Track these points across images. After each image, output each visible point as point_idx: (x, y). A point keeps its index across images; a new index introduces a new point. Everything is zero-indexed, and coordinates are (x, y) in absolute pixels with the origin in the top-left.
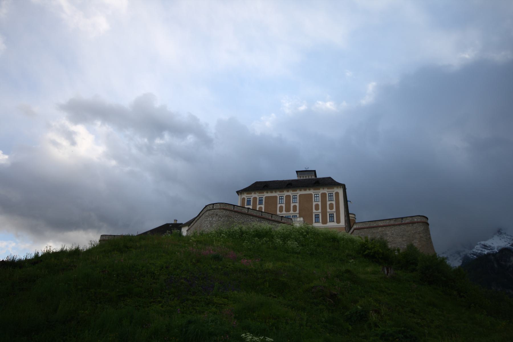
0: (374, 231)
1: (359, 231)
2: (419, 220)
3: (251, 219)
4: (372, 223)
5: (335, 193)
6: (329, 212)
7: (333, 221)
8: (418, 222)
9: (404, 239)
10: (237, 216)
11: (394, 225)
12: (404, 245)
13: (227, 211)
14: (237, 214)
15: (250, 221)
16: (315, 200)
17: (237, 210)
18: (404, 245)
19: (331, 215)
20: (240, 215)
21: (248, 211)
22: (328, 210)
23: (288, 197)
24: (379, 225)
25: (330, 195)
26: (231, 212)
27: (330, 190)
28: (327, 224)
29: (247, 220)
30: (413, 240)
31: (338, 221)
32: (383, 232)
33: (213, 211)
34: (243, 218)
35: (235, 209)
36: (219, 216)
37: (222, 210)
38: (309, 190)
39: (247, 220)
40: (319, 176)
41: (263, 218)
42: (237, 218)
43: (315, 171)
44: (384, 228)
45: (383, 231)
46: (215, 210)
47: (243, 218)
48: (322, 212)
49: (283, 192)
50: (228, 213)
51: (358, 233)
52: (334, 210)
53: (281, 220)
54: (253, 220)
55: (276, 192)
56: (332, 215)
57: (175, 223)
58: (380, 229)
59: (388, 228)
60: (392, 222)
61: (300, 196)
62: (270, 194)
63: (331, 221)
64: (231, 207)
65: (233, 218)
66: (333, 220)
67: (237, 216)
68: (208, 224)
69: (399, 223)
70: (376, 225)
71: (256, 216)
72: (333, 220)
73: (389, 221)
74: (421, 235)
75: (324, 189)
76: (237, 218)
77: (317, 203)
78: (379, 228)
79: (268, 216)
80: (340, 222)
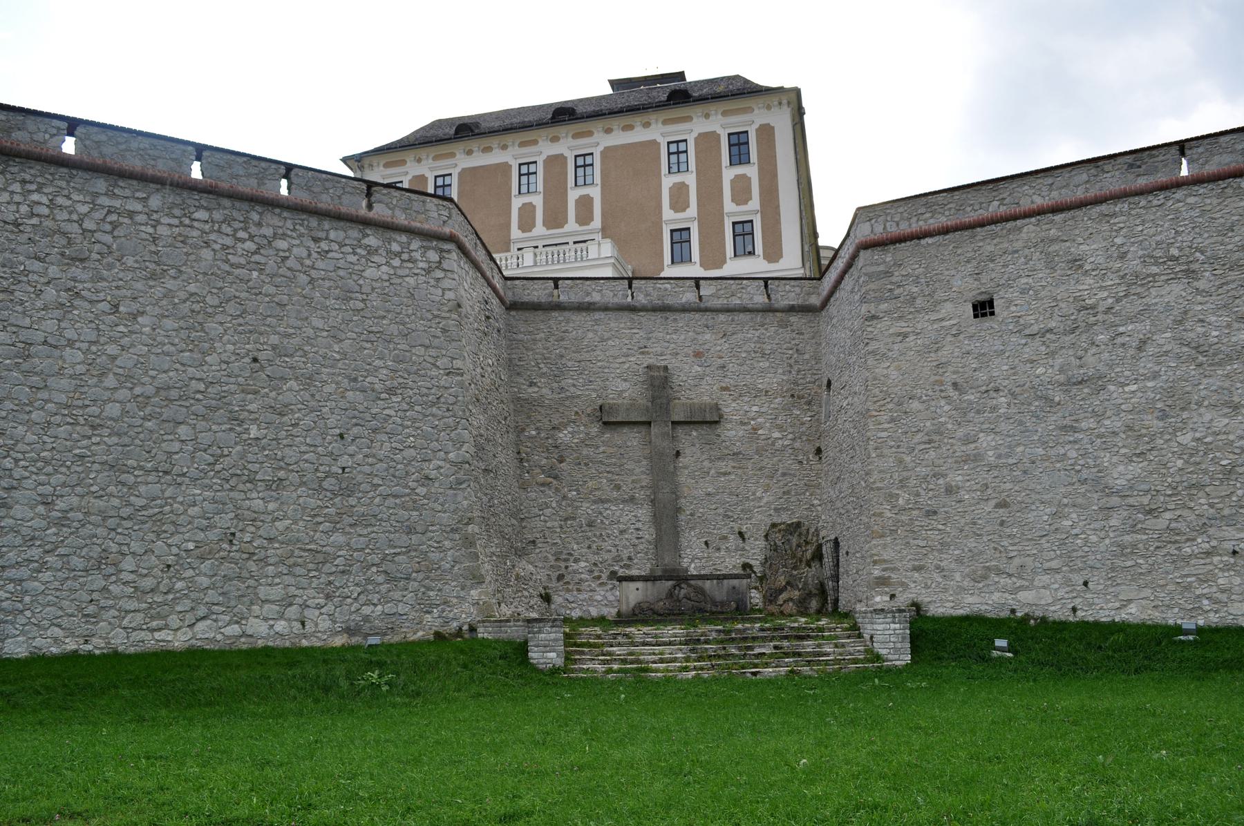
0: (990, 248)
6: (729, 215)
7: (752, 253)
15: (84, 209)
16: (669, 168)
22: (729, 206)
23: (556, 162)
27: (736, 123)
28: (725, 266)
31: (773, 253)
32: (1055, 247)
38: (647, 125)
40: (688, 79)
44: (1058, 218)
45: (1053, 241)
51: (881, 268)
52: (755, 203)
53: (370, 207)
56: (747, 227)
60: (1113, 181)
61: (606, 153)
62: (480, 160)
63: (740, 250)
66: (749, 248)
70: (1003, 209)
72: (749, 248)
73: (1093, 171)
75: (707, 116)
77: (677, 178)
78: (1019, 223)
79: (249, 176)
80: (781, 256)
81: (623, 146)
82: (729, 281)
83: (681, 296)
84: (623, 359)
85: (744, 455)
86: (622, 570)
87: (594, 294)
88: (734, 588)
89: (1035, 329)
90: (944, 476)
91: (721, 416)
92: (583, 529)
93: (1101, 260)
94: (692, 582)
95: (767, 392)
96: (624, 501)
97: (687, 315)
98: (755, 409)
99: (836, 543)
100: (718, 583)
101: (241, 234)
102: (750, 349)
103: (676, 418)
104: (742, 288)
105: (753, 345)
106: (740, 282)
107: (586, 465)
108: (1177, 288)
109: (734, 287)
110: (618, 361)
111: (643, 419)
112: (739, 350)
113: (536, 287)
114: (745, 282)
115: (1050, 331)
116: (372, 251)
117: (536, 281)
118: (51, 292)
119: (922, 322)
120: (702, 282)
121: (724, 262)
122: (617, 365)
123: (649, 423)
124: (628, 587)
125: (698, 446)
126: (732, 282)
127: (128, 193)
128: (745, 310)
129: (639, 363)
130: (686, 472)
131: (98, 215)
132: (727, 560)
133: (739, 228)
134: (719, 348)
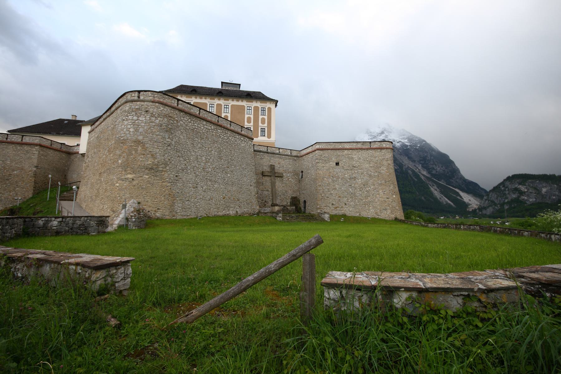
1: (322, 152)
2: (388, 146)
3: (204, 125)
4: (337, 144)
5: (268, 108)
6: (260, 126)
7: (264, 136)
8: (387, 148)
9: (371, 165)
10: (182, 119)
11: (361, 149)
12: (371, 171)
13: (166, 107)
14: (183, 115)
17: (183, 108)
18: (371, 171)
19: (262, 130)
20: (188, 118)
21: (200, 112)
22: (260, 124)
24: (345, 147)
25: (262, 109)
26: (173, 110)
27: (263, 105)
29: (198, 127)
30: (380, 167)
31: (269, 136)
32: (349, 156)
33: (138, 103)
34: (192, 122)
35: (179, 106)
36: (152, 113)
37: (157, 104)
38: (242, 101)
39: (198, 127)
41: (221, 126)
42: (184, 121)
43: (240, 85)
44: (351, 151)
45: (349, 154)
46: (142, 103)
47: (192, 122)
48: (254, 126)
49: (214, 99)
50: (167, 110)
52: (266, 125)
53: (241, 131)
54: (207, 127)
55: (206, 99)
57: (74, 119)
58: (346, 152)
59: (355, 152)
60: (359, 146)
61: (232, 106)
63: (262, 135)
64: (173, 102)
65: (177, 121)
66: (264, 135)
67: (182, 119)
68: (129, 127)
69: (367, 147)
71: (211, 122)
72: (264, 135)
74: (389, 162)
75: (257, 102)
76: (184, 121)
77: (249, 116)
78: (344, 150)
81: (237, 105)
89: (345, 169)
90: (330, 191)
91: (283, 175)
93: (357, 159)
96: (266, 191)
99: (305, 202)
101: (225, 135)
108: (367, 165)
115: (348, 169)
116: (242, 140)
118: (199, 145)
119: (327, 165)
121: (258, 137)
123: (271, 176)
127: (208, 125)
128: (287, 155)
131: (205, 129)
133: (262, 130)
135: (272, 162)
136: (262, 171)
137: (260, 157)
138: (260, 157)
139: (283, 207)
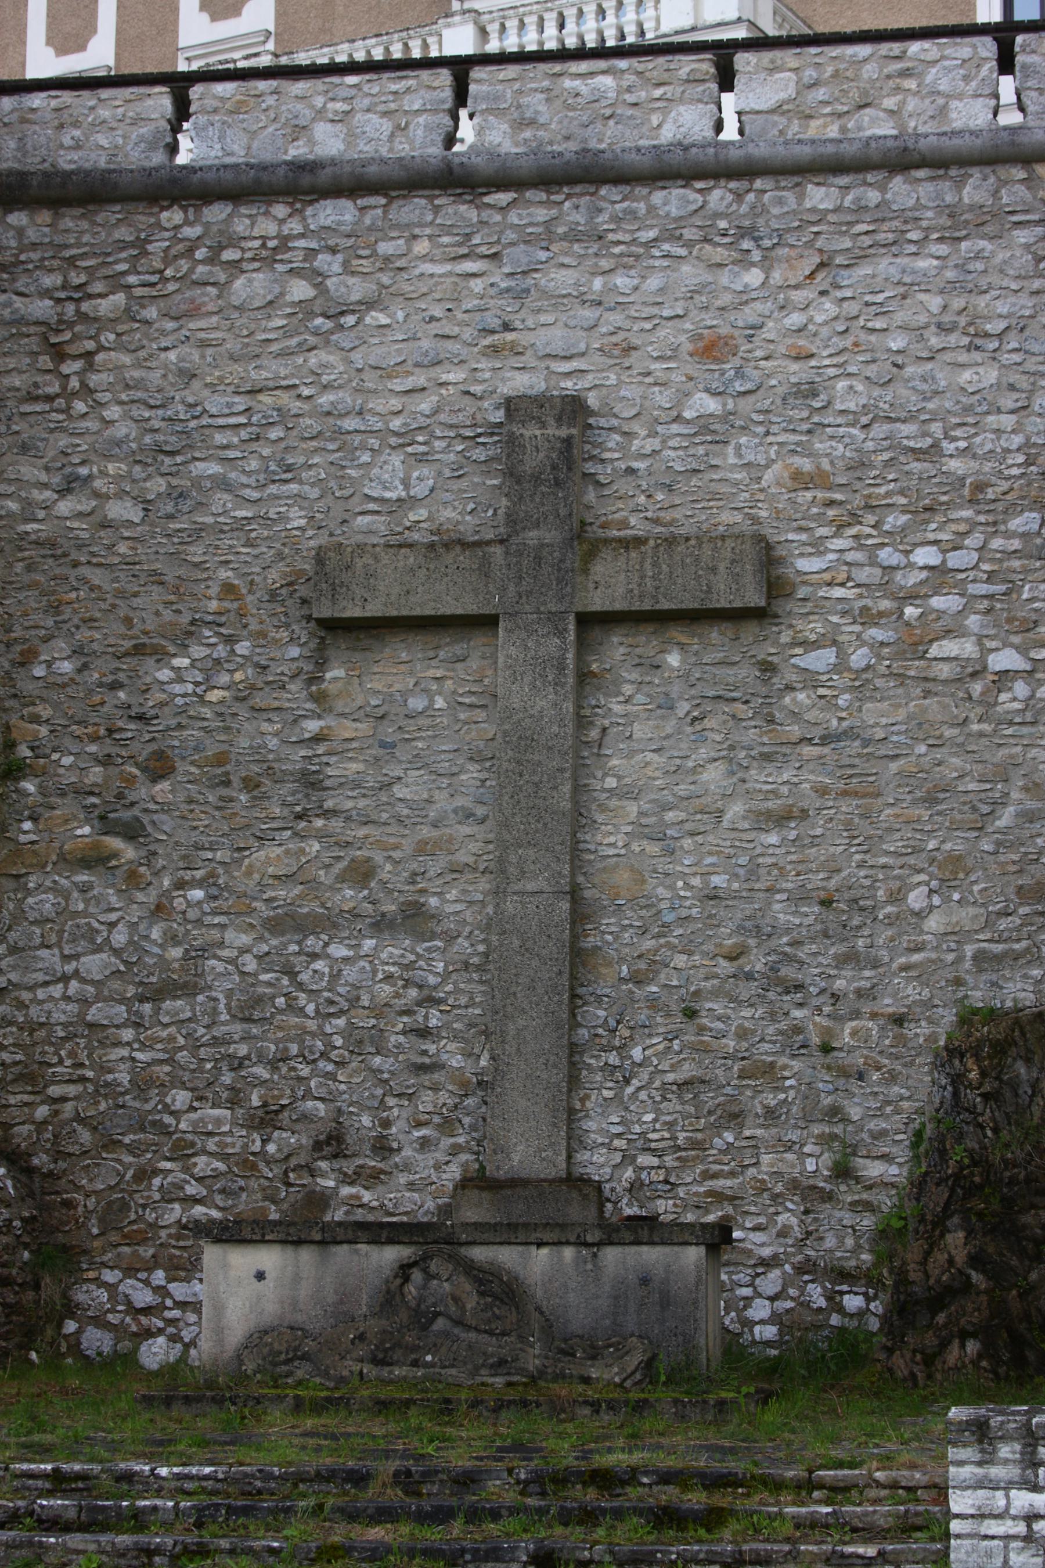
82: (850, 50)
83: (655, 120)
84: (420, 379)
85: (866, 743)
86: (346, 1191)
87: (322, 130)
88: (645, 1281)
92: (218, 1031)
94: (479, 1254)
95: (980, 487)
96: (381, 925)
97: (677, 192)
98: (926, 556)
100: (578, 1261)
102: (923, 319)
103: (598, 602)
104: (905, 73)
105: (935, 303)
106: (896, 47)
107: (250, 784)
109: (870, 71)
110: (398, 385)
111: (469, 606)
112: (878, 324)
113: (104, 113)
114: (915, 47)
117: (105, 93)
120: (742, 60)
122: (395, 403)
123: (487, 622)
124: (225, 1266)
125: (683, 707)
126: (863, 50)
129: (477, 389)
130: (632, 809)
132: (766, 1159)
134: (796, 319)
135: (554, 338)
136: (314, 541)
137: (300, 290)
138: (300, 290)
139: (391, 1255)
